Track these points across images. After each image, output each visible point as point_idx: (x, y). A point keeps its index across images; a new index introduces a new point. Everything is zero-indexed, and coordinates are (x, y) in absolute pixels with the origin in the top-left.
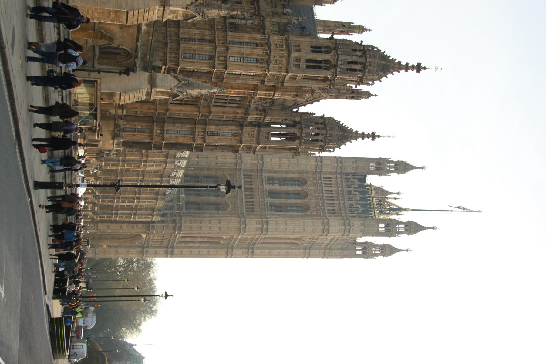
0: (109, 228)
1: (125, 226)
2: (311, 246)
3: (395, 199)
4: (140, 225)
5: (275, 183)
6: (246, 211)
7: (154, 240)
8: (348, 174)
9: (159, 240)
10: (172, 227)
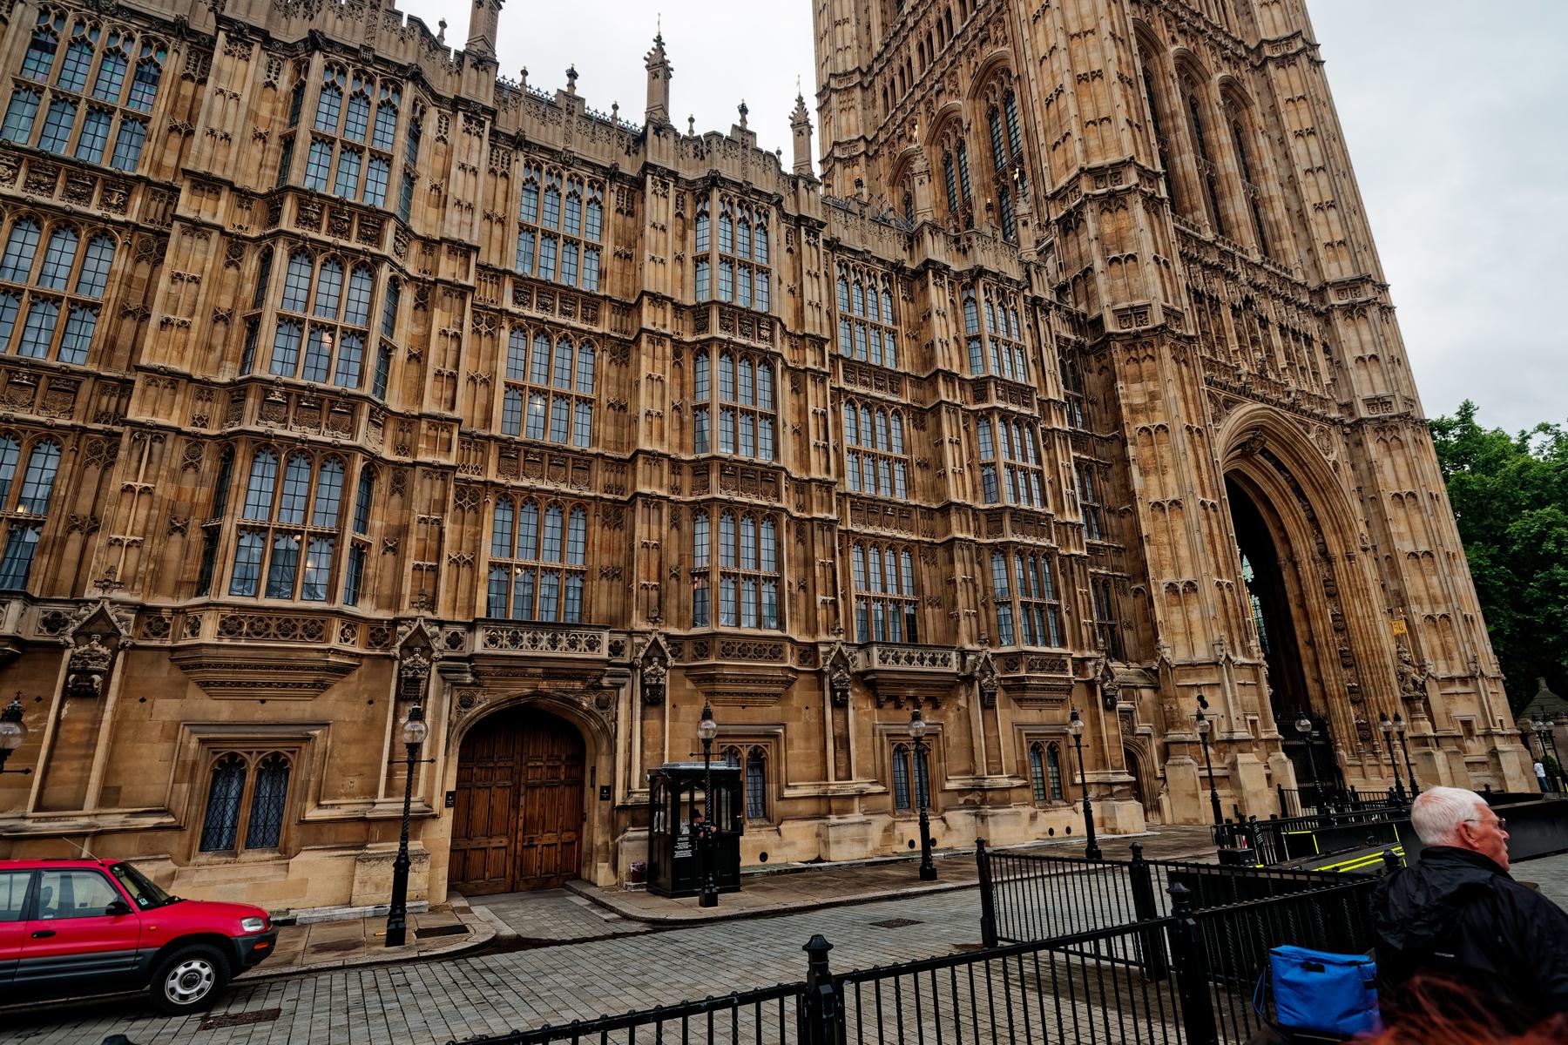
0: (1189, 583)
1: (1153, 480)
4: (1131, 393)
7: (1282, 363)
9: (1277, 341)
10: (1107, 216)
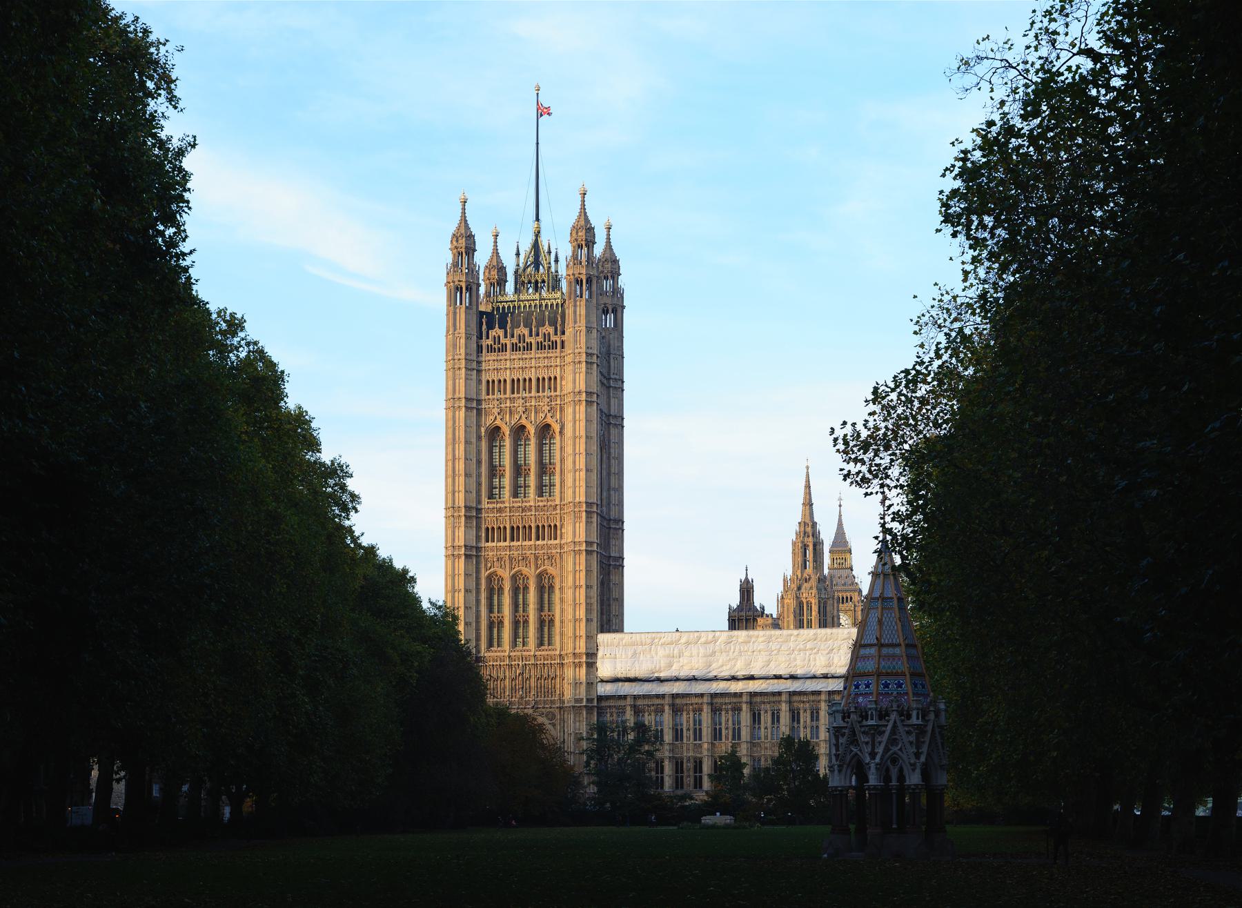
2: (605, 414)
3: (518, 254)
5: (500, 484)
6: (556, 539)
8: (479, 349)
